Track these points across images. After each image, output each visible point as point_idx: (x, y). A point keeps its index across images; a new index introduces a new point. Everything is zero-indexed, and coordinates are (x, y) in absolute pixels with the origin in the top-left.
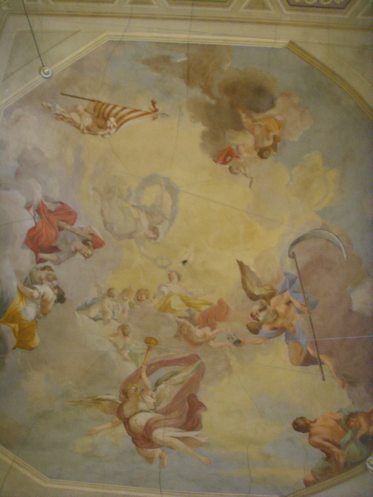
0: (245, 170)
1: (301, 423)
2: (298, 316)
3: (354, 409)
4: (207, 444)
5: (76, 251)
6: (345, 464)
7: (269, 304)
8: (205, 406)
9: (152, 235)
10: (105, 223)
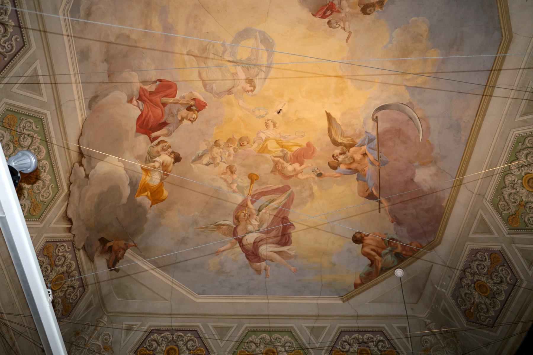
0: (344, 24)
1: (358, 236)
2: (370, 166)
3: (395, 237)
4: (295, 257)
5: (183, 119)
6: (382, 269)
7: (349, 151)
8: (293, 225)
9: (249, 88)
10: (205, 86)
